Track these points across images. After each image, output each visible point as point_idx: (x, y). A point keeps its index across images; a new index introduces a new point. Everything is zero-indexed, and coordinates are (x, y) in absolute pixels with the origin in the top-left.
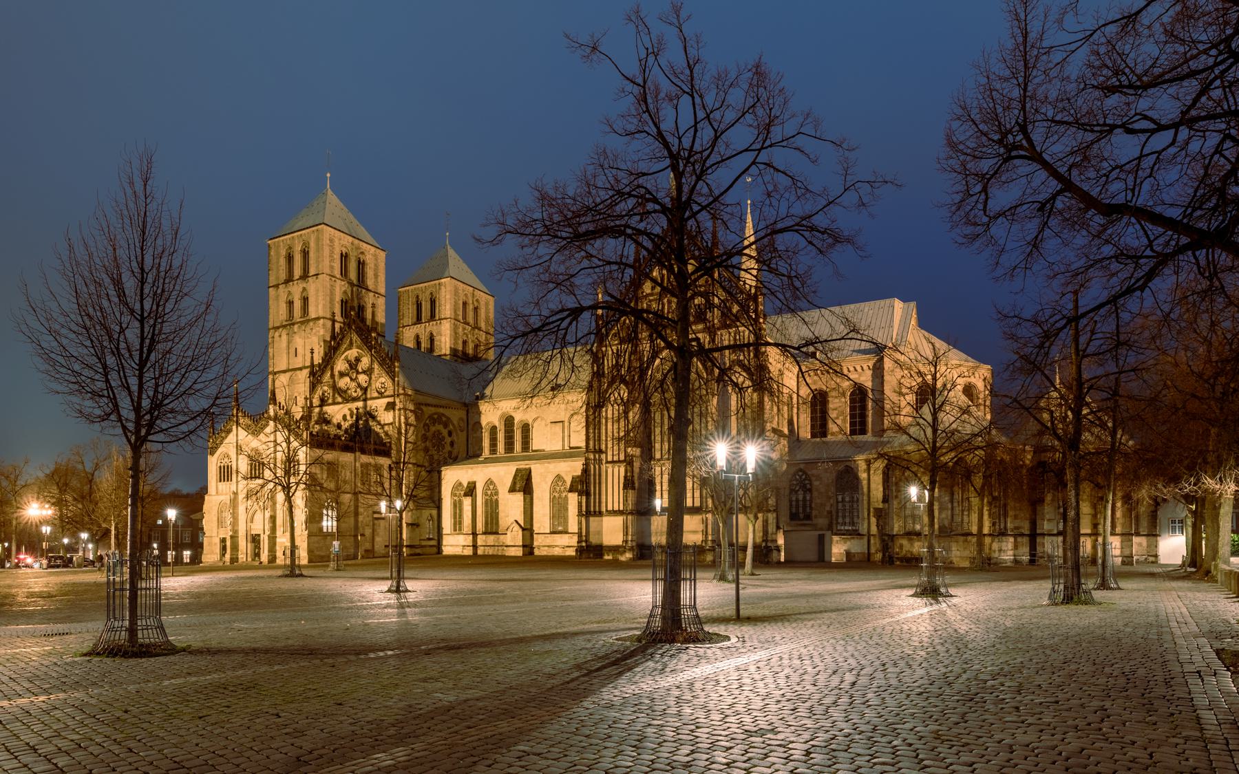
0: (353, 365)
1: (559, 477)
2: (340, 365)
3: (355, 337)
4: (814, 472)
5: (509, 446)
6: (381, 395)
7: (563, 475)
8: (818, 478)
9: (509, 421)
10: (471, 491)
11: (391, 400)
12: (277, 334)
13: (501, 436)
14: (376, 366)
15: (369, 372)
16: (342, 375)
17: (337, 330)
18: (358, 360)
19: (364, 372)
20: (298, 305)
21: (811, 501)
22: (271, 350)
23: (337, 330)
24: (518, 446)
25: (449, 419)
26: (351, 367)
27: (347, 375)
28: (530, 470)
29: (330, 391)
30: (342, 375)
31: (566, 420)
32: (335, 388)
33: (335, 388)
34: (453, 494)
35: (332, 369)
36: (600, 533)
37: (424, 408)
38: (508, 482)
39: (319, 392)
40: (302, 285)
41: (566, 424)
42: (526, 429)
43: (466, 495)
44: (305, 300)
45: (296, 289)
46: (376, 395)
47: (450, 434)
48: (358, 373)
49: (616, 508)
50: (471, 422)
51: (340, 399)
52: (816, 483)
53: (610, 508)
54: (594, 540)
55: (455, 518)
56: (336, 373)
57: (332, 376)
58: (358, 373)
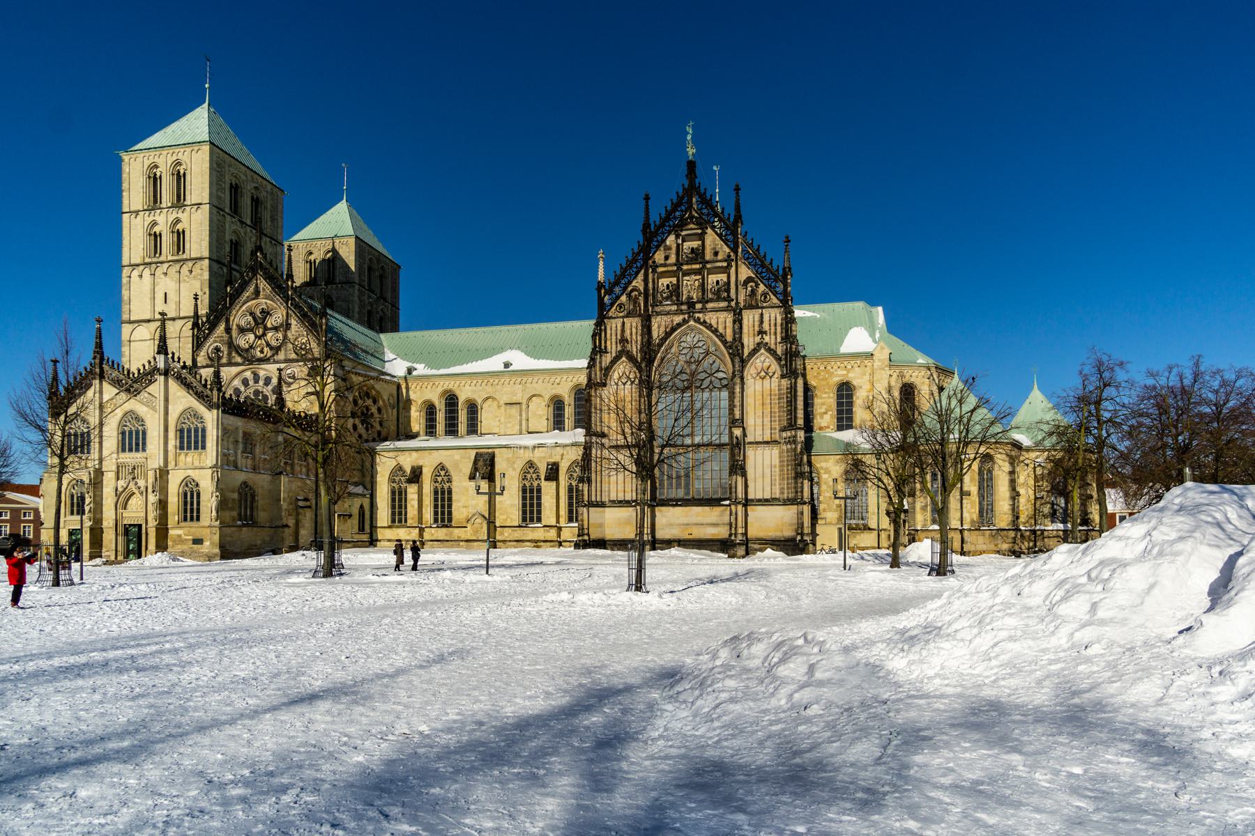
0: (260, 320)
1: (531, 464)
2: (239, 317)
3: (263, 284)
4: (823, 465)
7: (535, 461)
8: (828, 471)
10: (415, 476)
12: (136, 273)
13: (441, 417)
16: (242, 330)
18: (266, 313)
20: (167, 241)
21: (819, 494)
22: (125, 293)
24: (462, 427)
26: (257, 323)
27: (251, 330)
28: (492, 457)
29: (225, 349)
30: (242, 330)
32: (231, 345)
33: (231, 345)
34: (391, 480)
35: (228, 321)
36: (601, 525)
38: (467, 467)
40: (173, 215)
42: (473, 409)
43: (410, 481)
44: (180, 236)
45: (163, 220)
46: (293, 356)
47: (379, 410)
48: (266, 328)
49: (621, 498)
51: (239, 360)
52: (825, 476)
53: (613, 497)
54: (595, 535)
55: (393, 507)
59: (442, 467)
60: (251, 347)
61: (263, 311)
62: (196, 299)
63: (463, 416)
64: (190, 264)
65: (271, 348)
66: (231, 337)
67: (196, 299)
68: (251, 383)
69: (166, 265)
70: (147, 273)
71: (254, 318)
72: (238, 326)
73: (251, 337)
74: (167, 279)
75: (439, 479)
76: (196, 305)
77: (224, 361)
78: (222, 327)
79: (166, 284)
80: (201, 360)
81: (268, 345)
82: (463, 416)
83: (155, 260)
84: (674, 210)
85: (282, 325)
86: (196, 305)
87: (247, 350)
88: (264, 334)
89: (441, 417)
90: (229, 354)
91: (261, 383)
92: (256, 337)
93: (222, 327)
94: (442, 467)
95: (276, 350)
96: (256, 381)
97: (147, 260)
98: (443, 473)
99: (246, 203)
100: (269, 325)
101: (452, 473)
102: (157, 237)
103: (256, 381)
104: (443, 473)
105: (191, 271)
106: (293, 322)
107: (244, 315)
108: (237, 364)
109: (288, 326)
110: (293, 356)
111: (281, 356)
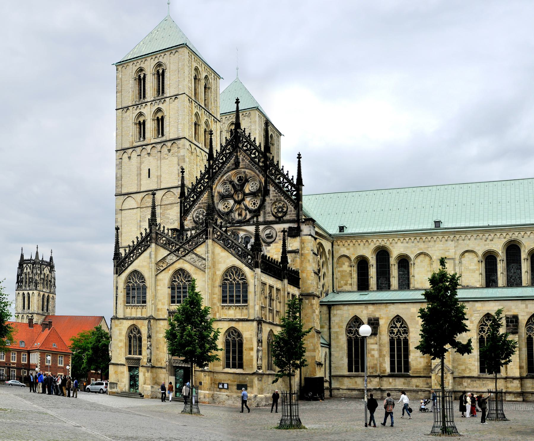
5: (384, 284)
6: (279, 220)
9: (383, 254)
11: (295, 225)
13: (373, 272)
14: (271, 188)
15: (263, 192)
16: (223, 197)
18: (244, 181)
19: (253, 194)
24: (394, 282)
25: (324, 249)
26: (236, 191)
27: (231, 196)
30: (223, 197)
31: (457, 257)
41: (457, 262)
48: (245, 195)
50: (336, 256)
58: (245, 195)
59: (398, 318)
60: (231, 211)
61: (240, 179)
62: (183, 172)
63: (394, 271)
65: (250, 211)
69: (150, 147)
70: (134, 155)
71: (233, 186)
72: (219, 193)
73: (232, 202)
74: (151, 158)
75: (395, 330)
76: (183, 178)
78: (206, 195)
79: (150, 162)
80: (188, 223)
81: (247, 208)
82: (394, 271)
83: (142, 143)
85: (259, 190)
86: (183, 178)
87: (228, 214)
88: (243, 200)
89: (373, 272)
92: (236, 202)
94: (398, 318)
97: (135, 144)
98: (398, 325)
100: (247, 191)
101: (410, 325)
102: (142, 125)
104: (398, 325)
106: (271, 188)
107: (224, 183)
109: (266, 193)
110: (272, 218)
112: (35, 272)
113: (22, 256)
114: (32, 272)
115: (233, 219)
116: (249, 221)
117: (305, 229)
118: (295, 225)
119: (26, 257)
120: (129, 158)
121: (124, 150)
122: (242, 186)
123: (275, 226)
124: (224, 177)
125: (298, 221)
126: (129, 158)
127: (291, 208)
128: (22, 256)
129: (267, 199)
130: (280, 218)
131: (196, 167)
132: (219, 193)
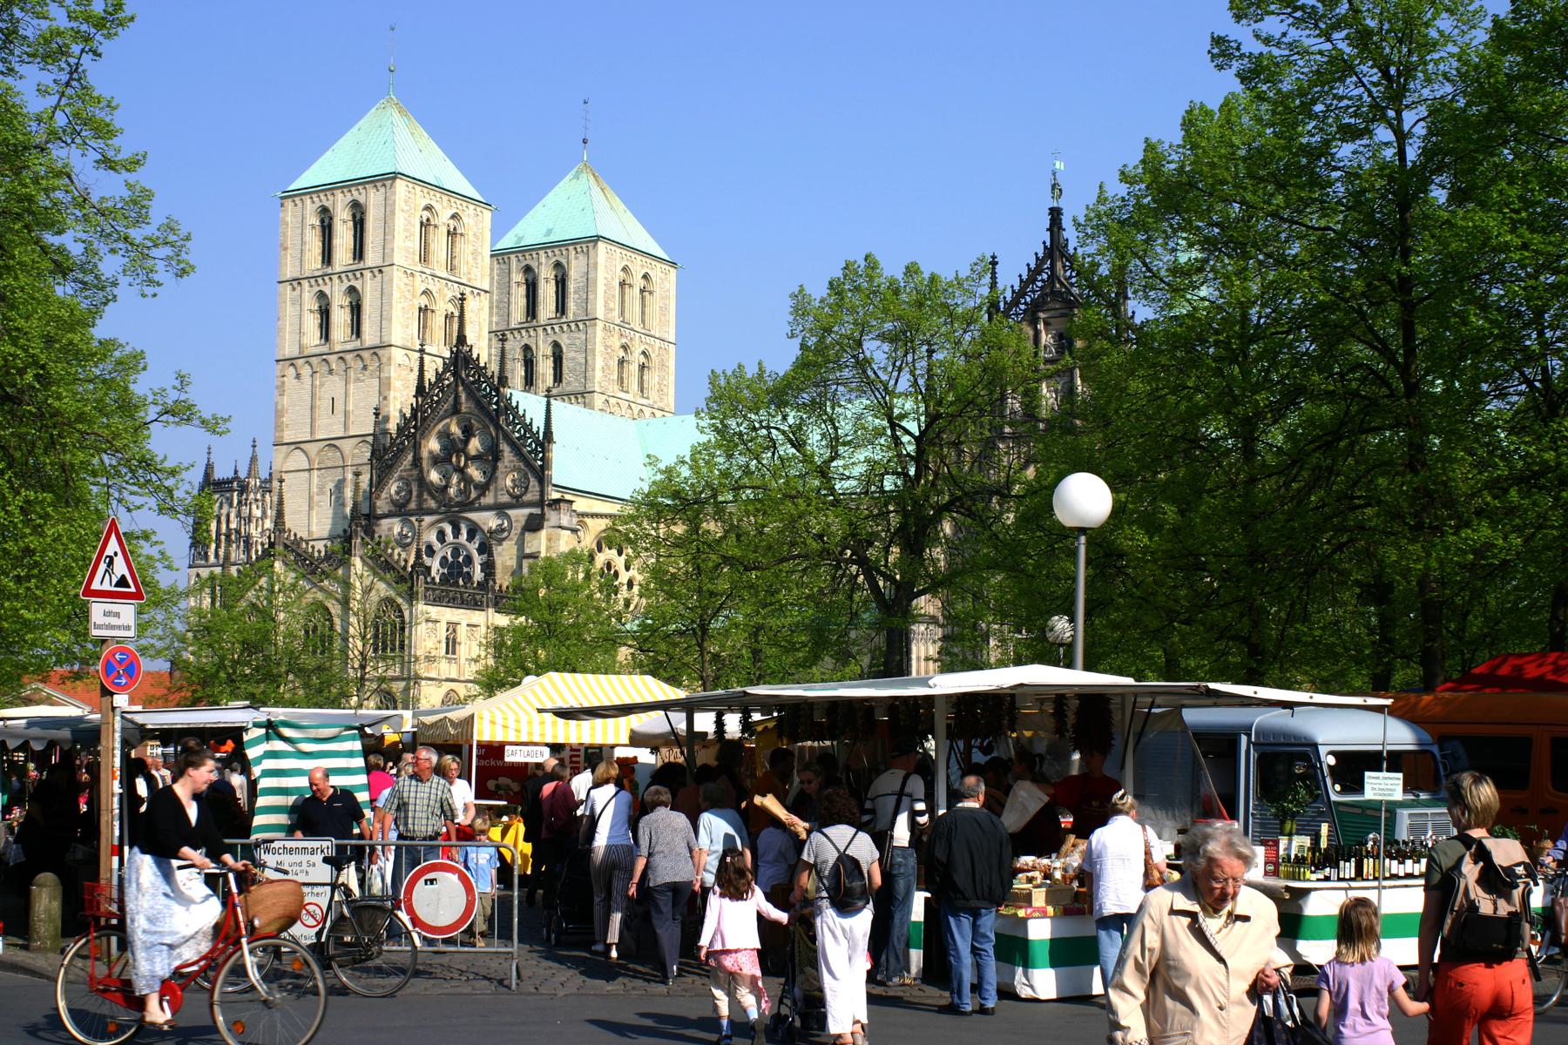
6: (517, 502)
11: (536, 511)
14: (505, 448)
15: (490, 458)
17: (430, 376)
18: (468, 432)
23: (430, 376)
30: (436, 461)
35: (417, 448)
37: (588, 520)
39: (393, 487)
51: (432, 504)
56: (425, 454)
57: (417, 461)
64: (366, 354)
66: (421, 471)
67: (377, 415)
68: (450, 537)
74: (335, 378)
77: (413, 505)
79: (332, 386)
84: (1032, 278)
90: (420, 496)
91: (464, 536)
93: (410, 457)
95: (483, 488)
96: (456, 533)
99: (439, 242)
103: (456, 533)
105: (365, 368)
106: (505, 448)
108: (431, 512)
110: (505, 499)
111: (488, 499)
112: (245, 510)
113: (209, 468)
114: (239, 515)
115: (451, 499)
116: (472, 503)
117: (551, 515)
118: (536, 511)
119: (220, 473)
120: (298, 376)
121: (291, 361)
122: (466, 442)
123: (511, 512)
124: (440, 426)
125: (540, 503)
126: (298, 376)
127: (533, 482)
128: (209, 468)
129: (500, 465)
130: (517, 497)
131: (401, 400)
132: (431, 452)
